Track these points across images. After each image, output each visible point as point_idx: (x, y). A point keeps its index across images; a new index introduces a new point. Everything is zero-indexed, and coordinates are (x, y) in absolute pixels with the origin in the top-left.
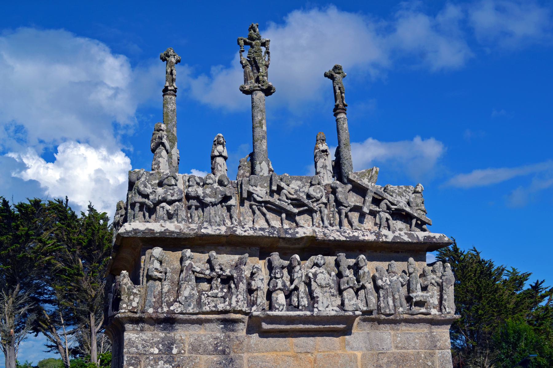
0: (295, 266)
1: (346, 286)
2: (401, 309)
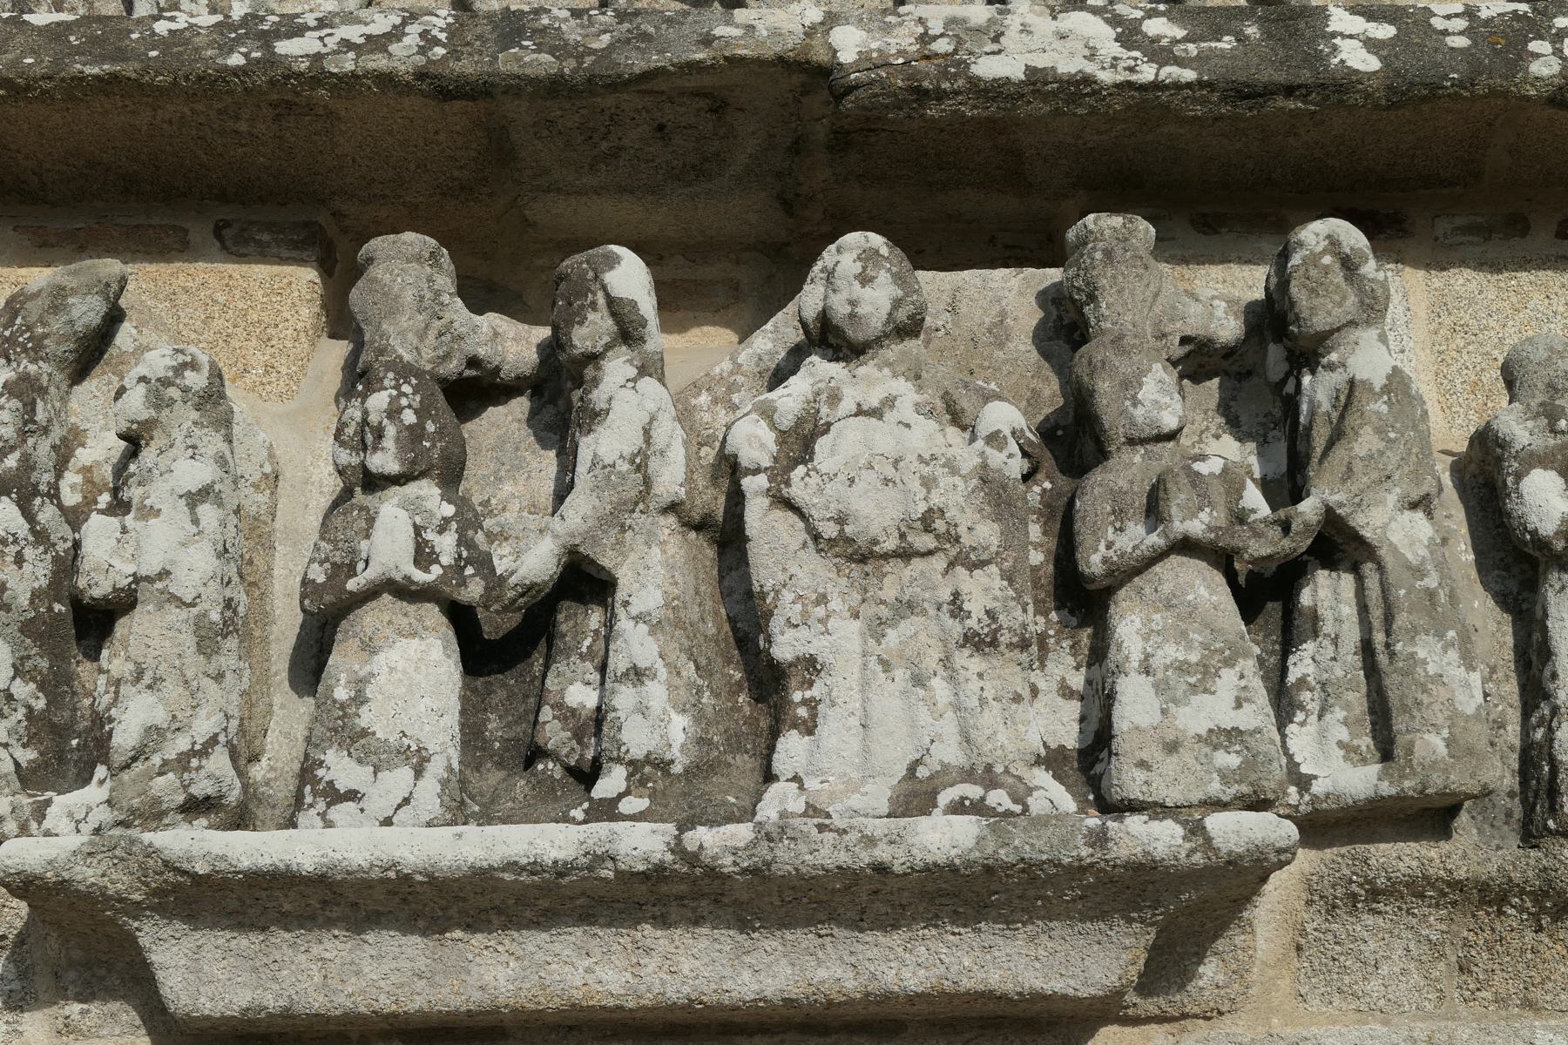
0: (593, 358)
1: (1135, 537)
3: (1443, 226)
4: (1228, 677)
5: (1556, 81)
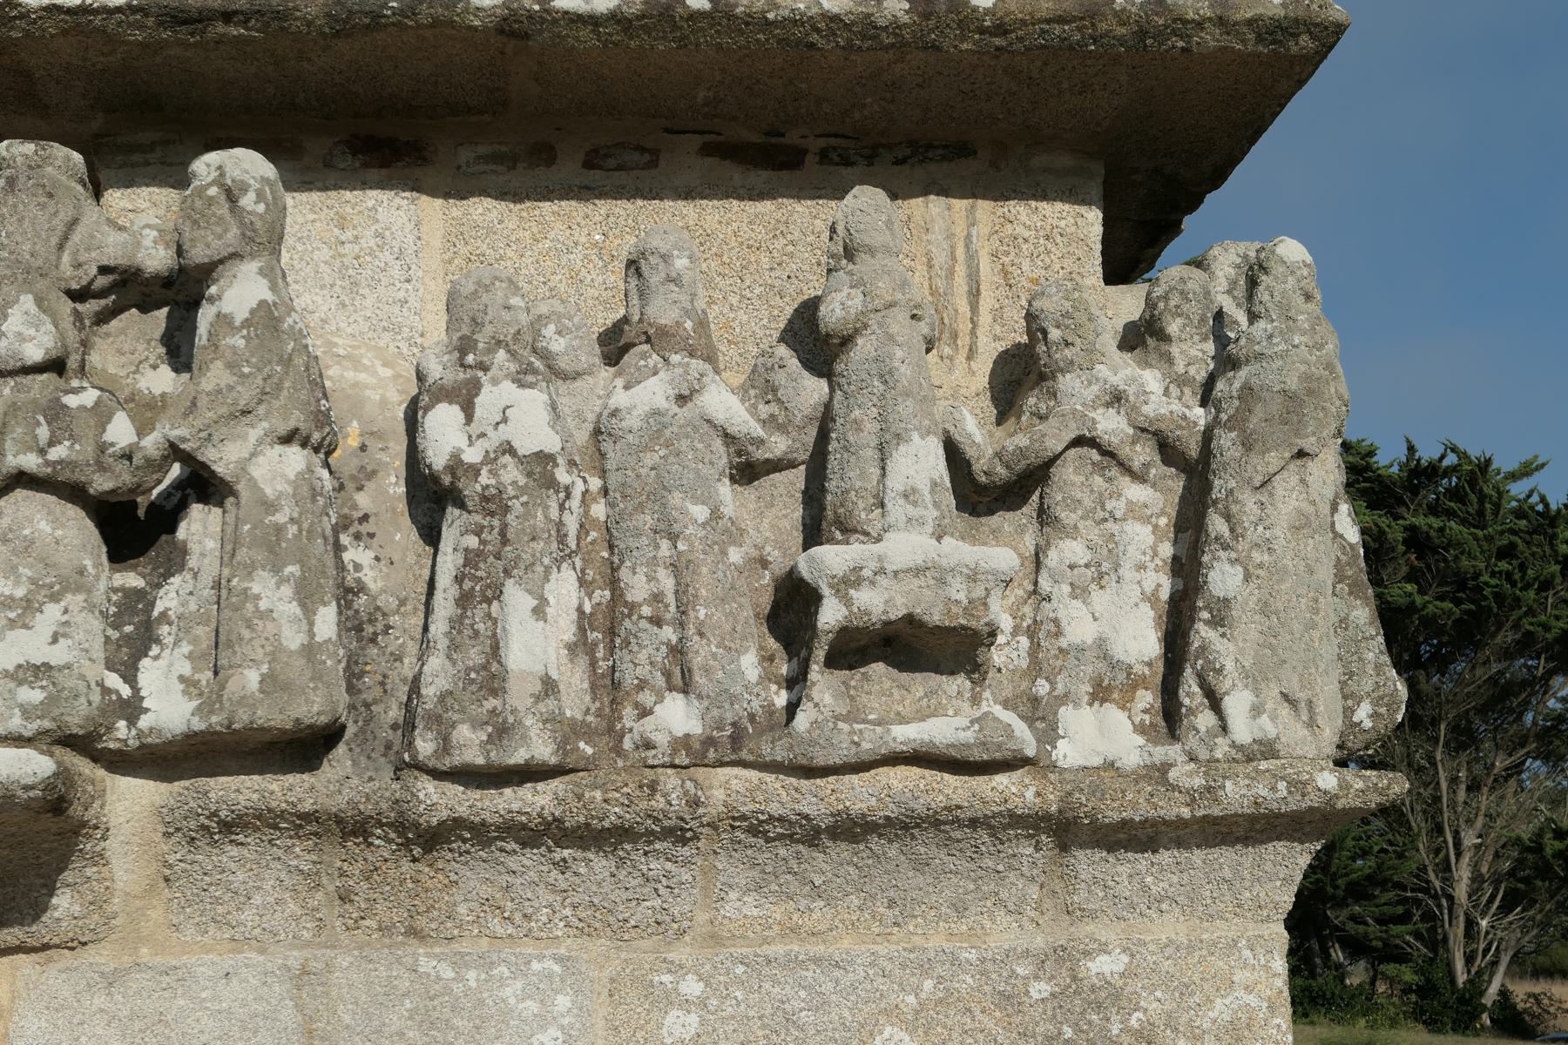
2: (676, 717)
3: (465, 155)
4: (53, 612)
5: (498, 11)
